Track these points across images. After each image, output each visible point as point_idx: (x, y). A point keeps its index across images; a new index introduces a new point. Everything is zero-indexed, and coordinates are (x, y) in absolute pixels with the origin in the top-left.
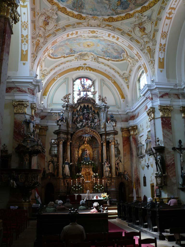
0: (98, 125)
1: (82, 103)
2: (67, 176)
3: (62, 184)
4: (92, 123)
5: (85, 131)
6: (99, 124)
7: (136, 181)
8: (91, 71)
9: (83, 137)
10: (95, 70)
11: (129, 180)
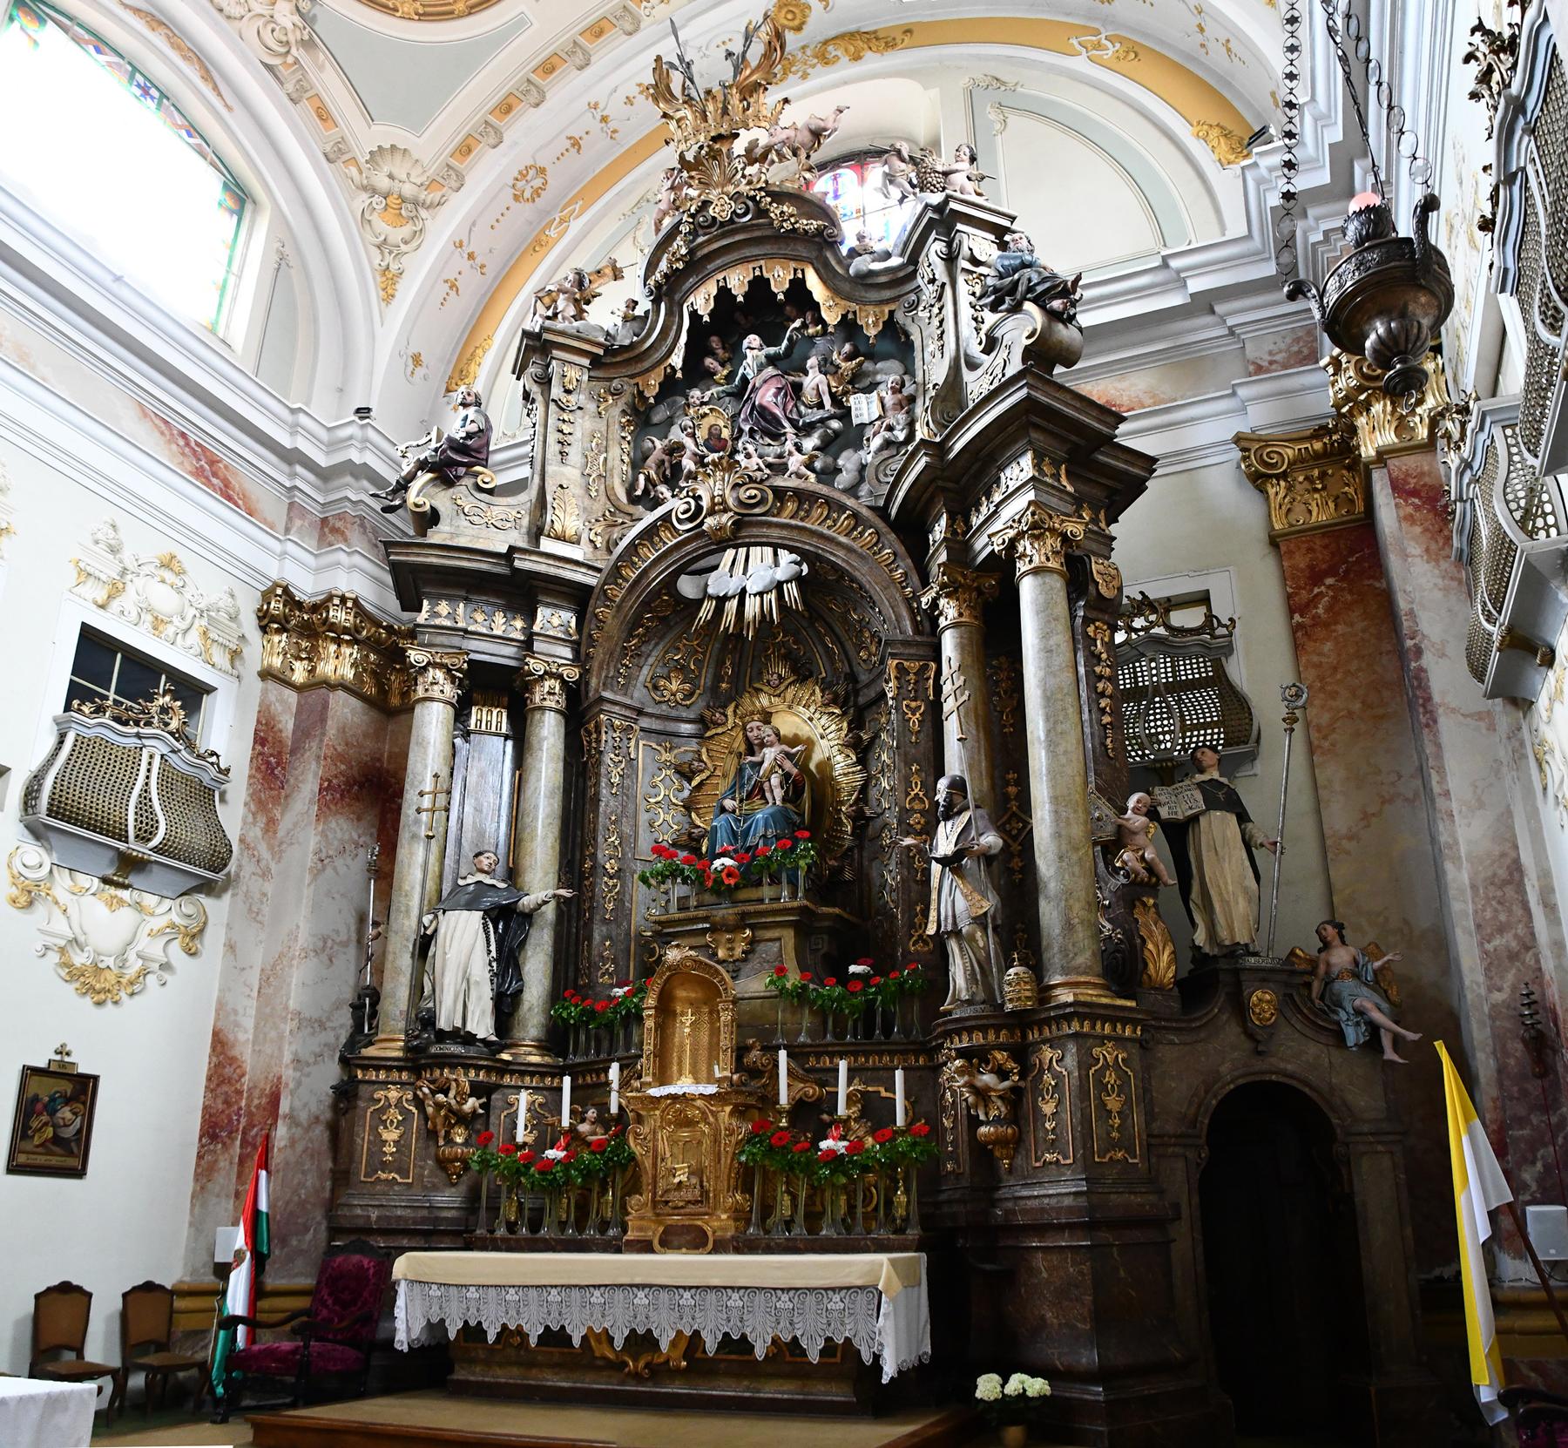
0: (888, 444)
1: (695, 267)
4: (836, 459)
5: (699, 508)
6: (901, 436)
7: (1517, 1048)
8: (873, 61)
9: (706, 611)
10: (908, 31)
11: (1397, 1041)
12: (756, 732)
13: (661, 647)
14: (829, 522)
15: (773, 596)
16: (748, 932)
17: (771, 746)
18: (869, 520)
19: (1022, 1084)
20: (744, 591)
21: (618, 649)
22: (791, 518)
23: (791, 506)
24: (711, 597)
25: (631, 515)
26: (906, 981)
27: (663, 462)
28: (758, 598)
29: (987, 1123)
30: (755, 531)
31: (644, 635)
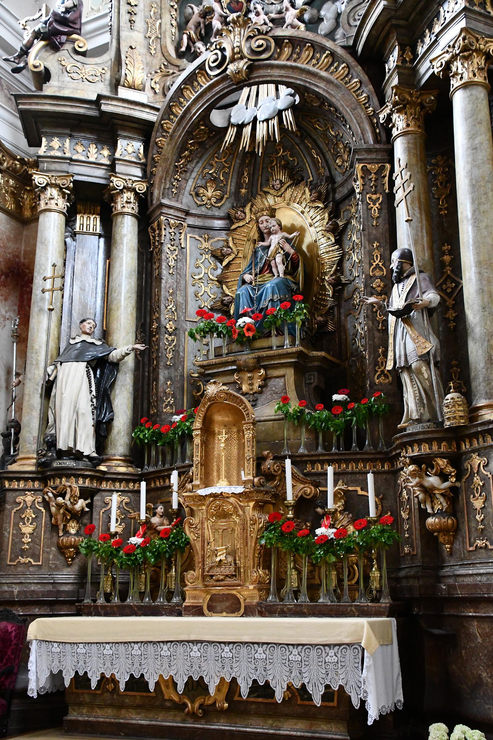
2: (61, 454)
3: (27, 529)
9: (231, 133)
12: (265, 224)
13: (200, 165)
14: (314, 61)
15: (275, 121)
16: (262, 371)
17: (276, 233)
18: (342, 57)
19: (458, 484)
20: (255, 119)
21: (172, 168)
22: (288, 60)
23: (287, 51)
24: (233, 125)
25: (178, 66)
26: (372, 406)
27: (199, 24)
28: (265, 123)
29: (433, 515)
30: (262, 72)
31: (189, 156)
